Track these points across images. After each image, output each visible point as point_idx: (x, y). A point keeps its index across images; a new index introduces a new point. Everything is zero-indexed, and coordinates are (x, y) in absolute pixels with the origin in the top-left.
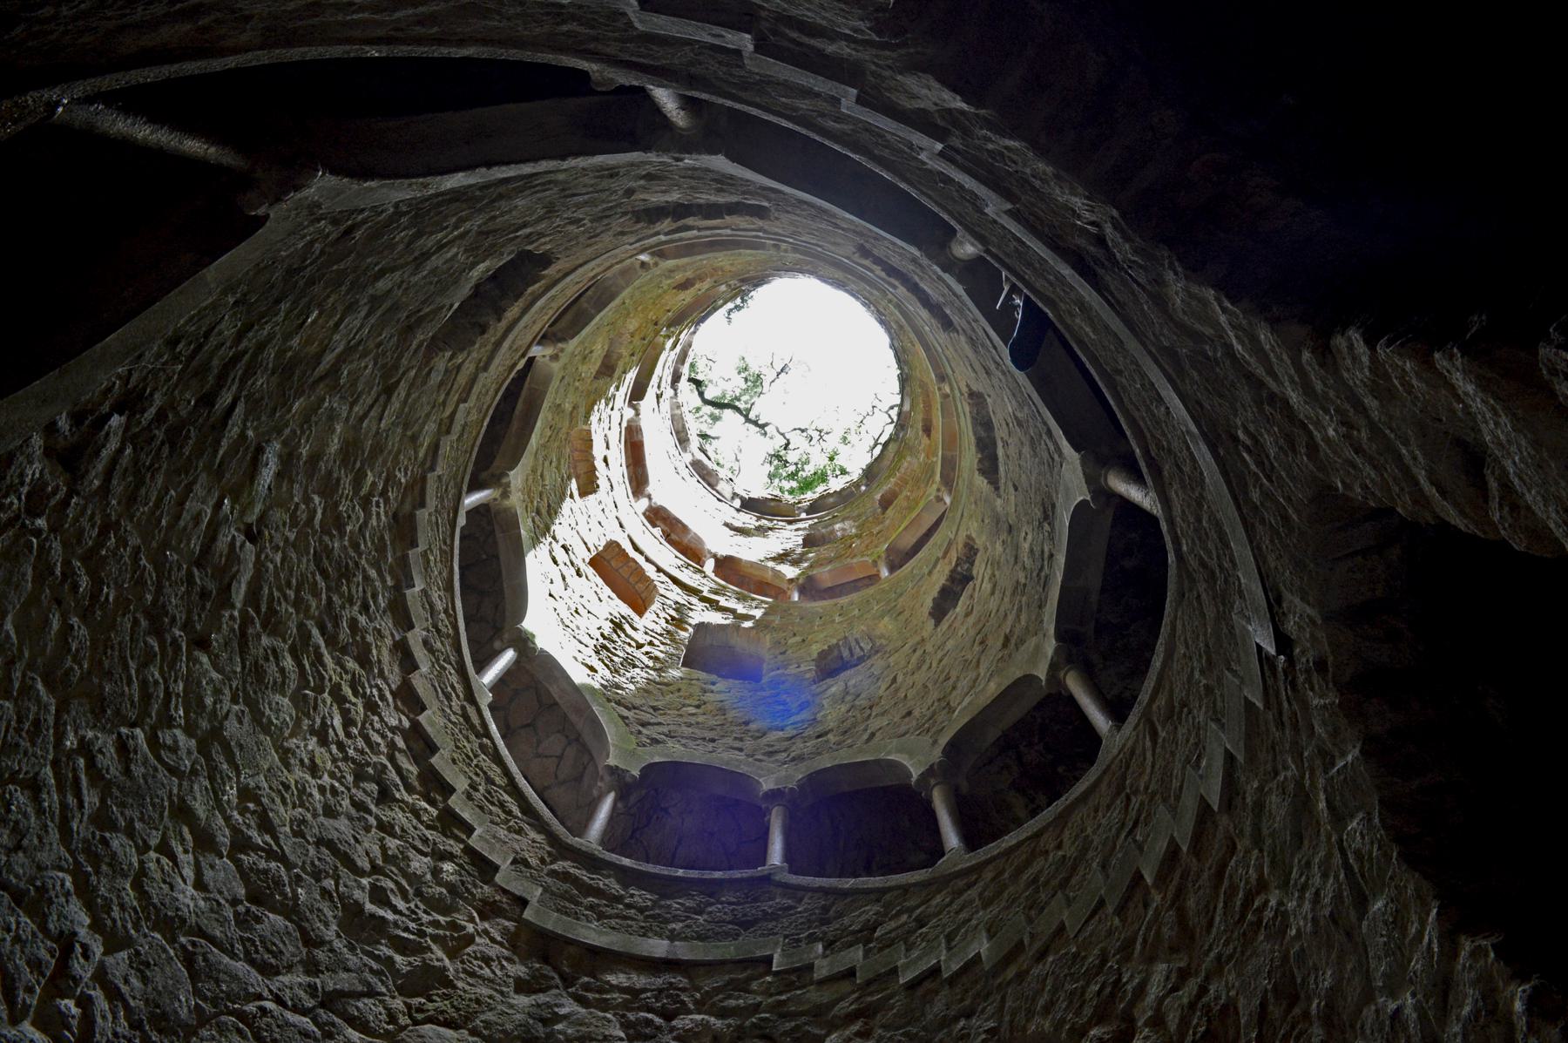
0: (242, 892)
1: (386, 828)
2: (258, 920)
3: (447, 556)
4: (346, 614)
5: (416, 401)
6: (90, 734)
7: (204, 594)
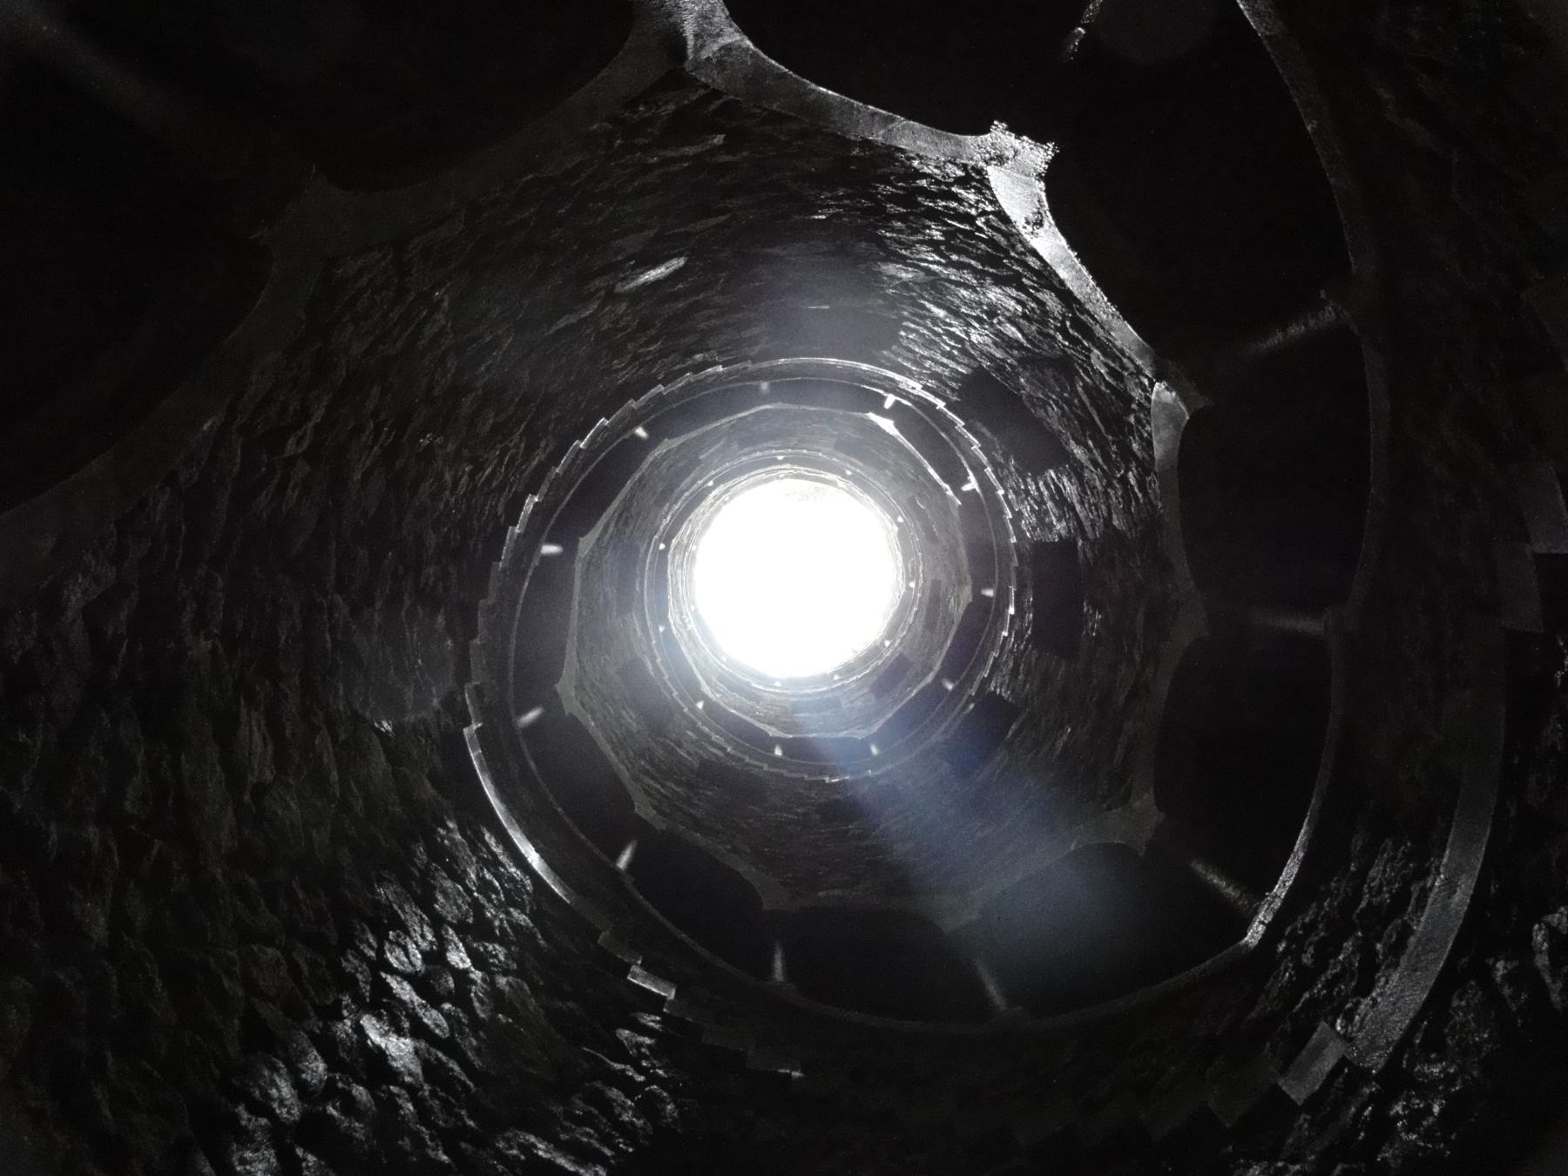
0: (372, 512)
6: (445, 304)
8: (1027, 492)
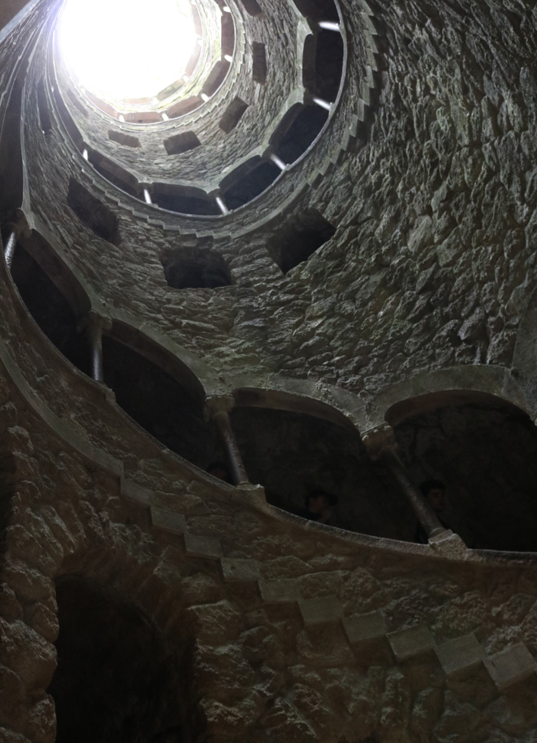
0: (485, 78)
1: (407, 30)
2: (481, 62)
3: (344, 99)
4: (401, 125)
5: (345, 200)
6: (519, 203)
7: (457, 207)
8: (148, 239)
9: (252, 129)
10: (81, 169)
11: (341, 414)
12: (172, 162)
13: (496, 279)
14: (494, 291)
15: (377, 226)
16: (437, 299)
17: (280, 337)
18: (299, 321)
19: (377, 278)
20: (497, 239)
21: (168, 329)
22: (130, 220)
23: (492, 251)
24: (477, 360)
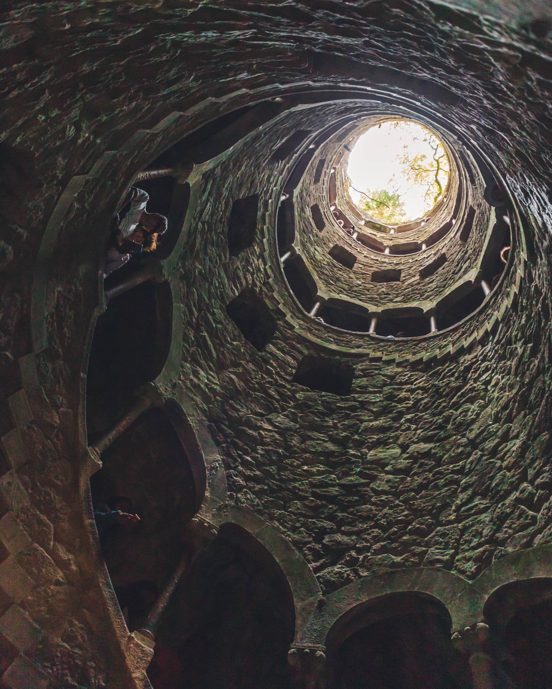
5: (375, 386)
6: (453, 508)
8: (252, 274)
9: (385, 294)
10: (270, 198)
11: (205, 489)
12: (325, 258)
13: (387, 534)
14: (376, 539)
15: (371, 421)
16: (343, 501)
17: (239, 407)
18: (262, 414)
19: (331, 447)
20: (417, 513)
21: (191, 325)
22: (258, 253)
23: (405, 516)
24: (312, 565)
